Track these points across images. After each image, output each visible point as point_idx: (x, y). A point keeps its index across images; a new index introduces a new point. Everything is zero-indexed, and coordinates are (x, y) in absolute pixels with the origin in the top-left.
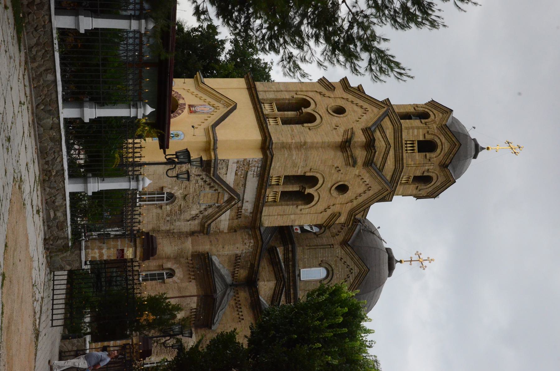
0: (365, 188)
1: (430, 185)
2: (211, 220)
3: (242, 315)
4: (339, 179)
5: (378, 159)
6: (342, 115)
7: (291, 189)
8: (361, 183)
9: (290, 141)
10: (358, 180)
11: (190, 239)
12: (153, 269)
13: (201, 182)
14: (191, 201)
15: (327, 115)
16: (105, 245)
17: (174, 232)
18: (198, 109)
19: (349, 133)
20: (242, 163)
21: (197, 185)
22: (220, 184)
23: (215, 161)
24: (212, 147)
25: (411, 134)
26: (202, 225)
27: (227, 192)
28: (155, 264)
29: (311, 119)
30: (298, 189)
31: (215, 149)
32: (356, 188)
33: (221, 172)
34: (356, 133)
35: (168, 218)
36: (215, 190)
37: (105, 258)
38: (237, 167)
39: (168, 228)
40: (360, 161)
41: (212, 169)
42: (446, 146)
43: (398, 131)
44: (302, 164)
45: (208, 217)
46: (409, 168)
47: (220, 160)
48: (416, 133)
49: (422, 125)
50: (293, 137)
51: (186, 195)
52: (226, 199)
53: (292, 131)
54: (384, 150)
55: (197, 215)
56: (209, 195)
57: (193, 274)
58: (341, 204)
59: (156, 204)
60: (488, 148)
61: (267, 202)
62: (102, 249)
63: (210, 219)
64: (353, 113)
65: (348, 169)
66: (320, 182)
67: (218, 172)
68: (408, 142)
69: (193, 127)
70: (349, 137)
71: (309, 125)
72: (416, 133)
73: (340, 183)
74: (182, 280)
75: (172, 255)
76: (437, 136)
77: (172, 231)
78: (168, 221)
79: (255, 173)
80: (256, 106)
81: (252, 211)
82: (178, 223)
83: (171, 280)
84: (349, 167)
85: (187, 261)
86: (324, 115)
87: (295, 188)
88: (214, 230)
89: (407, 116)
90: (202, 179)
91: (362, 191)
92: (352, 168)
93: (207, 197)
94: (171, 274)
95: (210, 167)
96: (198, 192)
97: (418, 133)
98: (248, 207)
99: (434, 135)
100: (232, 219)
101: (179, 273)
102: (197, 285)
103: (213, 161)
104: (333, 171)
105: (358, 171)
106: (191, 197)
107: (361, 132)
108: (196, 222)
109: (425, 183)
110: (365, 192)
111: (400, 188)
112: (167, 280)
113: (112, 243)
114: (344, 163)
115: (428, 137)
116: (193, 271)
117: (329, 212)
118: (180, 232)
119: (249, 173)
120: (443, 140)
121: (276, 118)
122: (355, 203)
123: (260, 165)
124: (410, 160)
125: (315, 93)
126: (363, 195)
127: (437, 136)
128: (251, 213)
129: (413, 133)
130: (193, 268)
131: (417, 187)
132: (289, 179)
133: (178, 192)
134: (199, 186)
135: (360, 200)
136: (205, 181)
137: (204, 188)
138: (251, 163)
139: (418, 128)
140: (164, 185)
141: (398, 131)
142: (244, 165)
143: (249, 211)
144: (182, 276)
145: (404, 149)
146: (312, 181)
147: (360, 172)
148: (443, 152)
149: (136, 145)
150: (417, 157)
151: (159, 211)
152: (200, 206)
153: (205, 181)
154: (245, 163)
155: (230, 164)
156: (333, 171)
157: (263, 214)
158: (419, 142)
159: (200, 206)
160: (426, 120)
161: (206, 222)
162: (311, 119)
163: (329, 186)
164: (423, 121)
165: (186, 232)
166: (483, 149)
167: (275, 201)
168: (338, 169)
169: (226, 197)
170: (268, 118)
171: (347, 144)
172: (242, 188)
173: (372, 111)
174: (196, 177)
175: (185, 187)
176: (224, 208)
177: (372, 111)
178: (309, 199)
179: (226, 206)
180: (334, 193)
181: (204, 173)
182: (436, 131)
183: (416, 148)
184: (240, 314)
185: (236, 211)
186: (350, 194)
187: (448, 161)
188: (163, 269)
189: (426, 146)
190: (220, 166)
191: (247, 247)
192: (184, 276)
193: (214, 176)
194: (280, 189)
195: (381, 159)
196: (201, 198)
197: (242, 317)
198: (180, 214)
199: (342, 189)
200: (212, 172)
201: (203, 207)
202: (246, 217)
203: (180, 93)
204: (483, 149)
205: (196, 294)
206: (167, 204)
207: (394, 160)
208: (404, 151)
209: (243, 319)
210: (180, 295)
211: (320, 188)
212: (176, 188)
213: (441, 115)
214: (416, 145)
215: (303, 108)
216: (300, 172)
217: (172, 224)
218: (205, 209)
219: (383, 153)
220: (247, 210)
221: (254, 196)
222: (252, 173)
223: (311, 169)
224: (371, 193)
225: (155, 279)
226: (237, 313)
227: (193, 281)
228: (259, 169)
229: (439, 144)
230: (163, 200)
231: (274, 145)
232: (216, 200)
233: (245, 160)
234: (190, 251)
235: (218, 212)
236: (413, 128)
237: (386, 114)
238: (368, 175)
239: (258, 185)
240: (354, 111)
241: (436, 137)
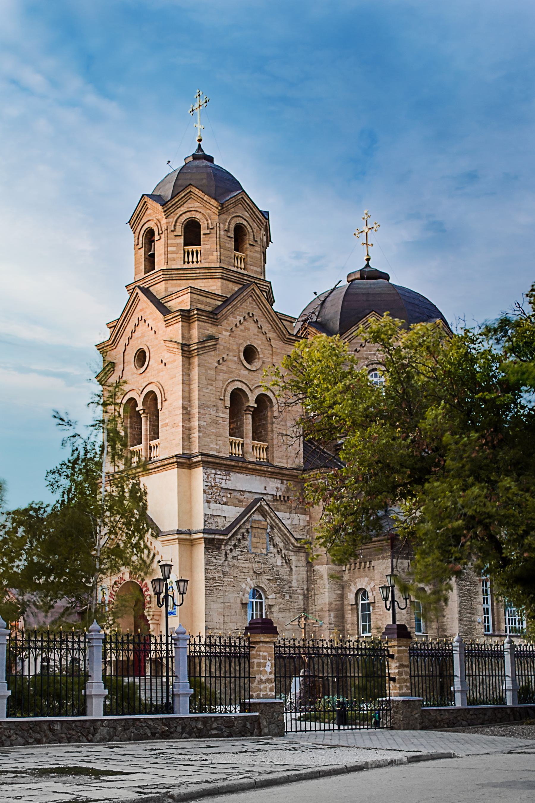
0: (250, 320)
1: (248, 227)
2: (291, 538)
4: (236, 359)
5: (208, 304)
6: (147, 355)
7: (250, 427)
8: (242, 327)
9: (181, 429)
10: (237, 331)
11: (316, 567)
12: (356, 619)
14: (263, 565)
15: (148, 375)
16: (257, 676)
17: (307, 589)
19: (170, 345)
20: (209, 496)
21: (239, 557)
22: (238, 526)
23: (206, 533)
24: (187, 537)
25: (174, 256)
26: (298, 550)
27: (251, 516)
28: (350, 616)
29: (151, 397)
30: (250, 417)
31: (190, 533)
32: (251, 335)
33: (222, 524)
34: (172, 336)
35: (287, 597)
36: (248, 532)
37: (272, 677)
38: (216, 502)
39: (301, 597)
40: (211, 330)
41: (217, 537)
42: (192, 205)
43: (169, 275)
44: (213, 413)
45: (286, 541)
46: (222, 258)
47: (205, 526)
48: (174, 249)
49: (163, 239)
50: (175, 425)
51: (254, 572)
52: (261, 518)
53: (166, 425)
54: (195, 296)
55: (283, 558)
56: (254, 540)
58: (272, 355)
59: (266, 613)
60: (200, 140)
61: (267, 459)
62: (261, 679)
63: (290, 540)
65: (222, 347)
66: (239, 385)
67: (222, 529)
68: (186, 260)
70: (176, 346)
71: (159, 401)
72: (174, 249)
73: (242, 358)
74: (372, 579)
75: (339, 592)
76: (178, 218)
77: (306, 592)
78: (290, 597)
79: (225, 478)
81: (280, 481)
82: (294, 584)
83: (370, 595)
84: (218, 346)
85: (347, 572)
86: (146, 379)
87: (248, 420)
88: (305, 533)
89: (150, 260)
90: (231, 550)
91: (255, 325)
92: (220, 341)
93: (256, 543)
94: (362, 593)
95: (214, 539)
96: (250, 556)
97: (173, 245)
98: (273, 486)
99: (176, 222)
100: (290, 508)
101: (362, 583)
102: (379, 559)
103: (206, 536)
104: (224, 368)
105: (224, 333)
106: (257, 566)
107: (170, 328)
108: (293, 558)
109: (245, 235)
110: (256, 322)
111: (253, 271)
112: (371, 599)
113: (255, 669)
114: (213, 353)
115: (179, 230)
116: (360, 563)
118: (307, 581)
119: (223, 485)
120: (183, 209)
121: (150, 447)
122: (271, 335)
123: (213, 471)
124: (211, 257)
126: (259, 323)
127: (178, 218)
128: (282, 483)
129: (173, 252)
130: (356, 564)
131: (250, 244)
132: (235, 430)
133: (250, 583)
134: (241, 555)
135: (266, 327)
136: (235, 546)
137: (244, 548)
138: (209, 484)
139: (167, 245)
140: (239, 601)
141: (169, 275)
142: (212, 493)
143: (279, 485)
144: (366, 579)
145: (195, 265)
146: (237, 396)
147: (226, 330)
148: (200, 210)
149: (158, 641)
150: (208, 247)
151: (274, 609)
152: (271, 553)
153: (235, 546)
154: (210, 491)
155: (210, 512)
156: (224, 368)
157: (285, 465)
158: (186, 244)
159: (271, 553)
160: (156, 233)
161: (293, 544)
162: (151, 397)
163: (246, 372)
164: (156, 237)
165: (307, 572)
166: (200, 148)
167: (267, 449)
168: (221, 361)
169: (257, 517)
170: (150, 458)
171: (186, 349)
172: (246, 495)
173: (141, 310)
174: (228, 559)
175: (242, 574)
176: (274, 520)
177: (141, 310)
178: (262, 400)
179: (271, 517)
180: (256, 364)
181: (223, 547)
182: (171, 220)
183: (195, 248)
185: (279, 503)
186: (258, 343)
187: (213, 202)
188: (357, 604)
189: (192, 233)
190: (213, 527)
192: (366, 576)
193: (227, 535)
194: (249, 441)
195: (208, 300)
196: (259, 551)
198: (282, 580)
199: (250, 353)
200: (221, 537)
201: (272, 548)
202: (288, 489)
204: (200, 148)
205: (390, 560)
206: (267, 598)
207: (210, 280)
208: (198, 265)
211: (248, 386)
212: (244, 586)
213: (149, 212)
214: (190, 248)
215: (137, 409)
216: (226, 415)
217: (295, 592)
218: (275, 546)
219: (200, 298)
220: (277, 488)
221: (258, 478)
222: (224, 481)
223: (221, 399)
224: (257, 312)
225: (369, 615)
227: (373, 563)
228: (218, 472)
229: (188, 215)
230: (261, 603)
231: (186, 452)
232: (263, 531)
233: (205, 492)
234: (334, 566)
235: (280, 528)
236: (166, 253)
237: (147, 292)
238: (231, 318)
239: (242, 473)
240: (143, 336)
241: (179, 220)
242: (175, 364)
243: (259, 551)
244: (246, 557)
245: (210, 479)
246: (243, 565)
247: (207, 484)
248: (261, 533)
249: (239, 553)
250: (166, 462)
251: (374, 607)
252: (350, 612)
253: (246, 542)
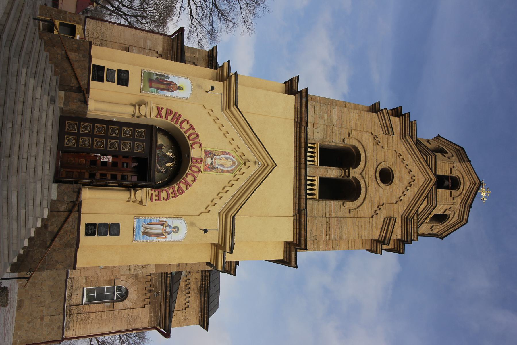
3: (189, 302)
18: (218, 161)
28: (105, 279)
57: (149, 295)
64: (398, 181)
69: (205, 231)
74: (134, 303)
80: (300, 169)
94: (123, 296)
101: (133, 295)
102: (150, 312)
125: (369, 134)
144: (135, 297)
184: (187, 300)
192: (138, 297)
197: (188, 304)
203: (197, 130)
209: (188, 307)
210: (130, 328)
215: (351, 168)
226: (185, 297)
242: (374, 230)
250: (303, 231)
251: (109, 307)
252: (108, 279)
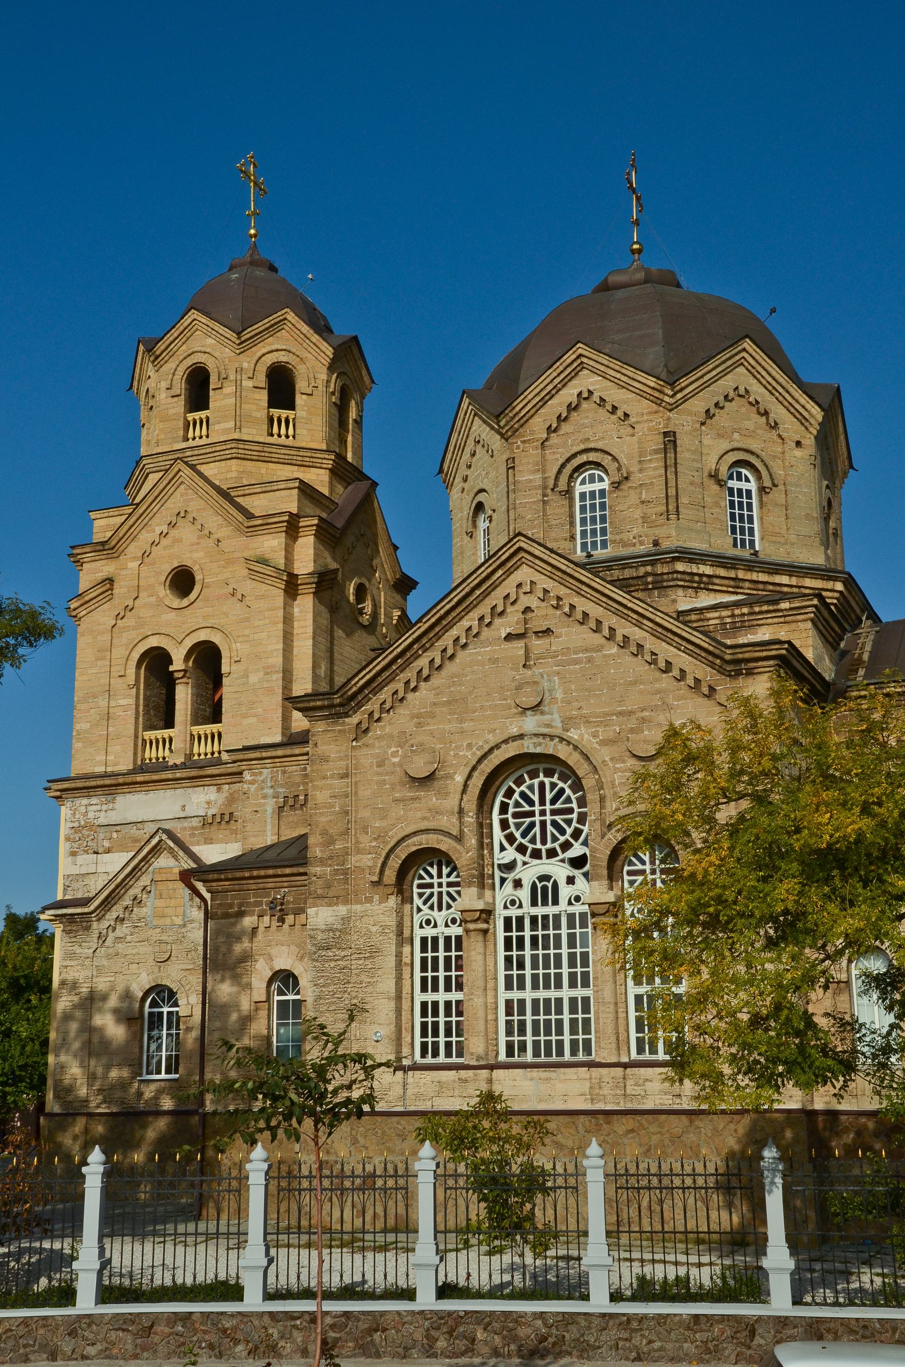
13: (122, 930)
20: (76, 845)
38: (86, 852)
56: (160, 903)
79: (104, 807)
81: (213, 789)
96: (150, 932)
117: (248, 586)
119: (103, 820)
128: (219, 790)
136: (120, 920)
138: (76, 825)
146: (156, 661)
147: (135, 559)
152: (192, 921)
154: (77, 836)
159: (192, 921)
181: (95, 925)
185: (215, 827)
191: (253, 788)
196: (168, 921)
199: (183, 581)
228: (94, 800)
243: (168, 921)
244: (143, 936)
245: (77, 816)
246: (134, 952)
247: (71, 825)
248: (174, 889)
249: (127, 931)
253: (144, 910)
